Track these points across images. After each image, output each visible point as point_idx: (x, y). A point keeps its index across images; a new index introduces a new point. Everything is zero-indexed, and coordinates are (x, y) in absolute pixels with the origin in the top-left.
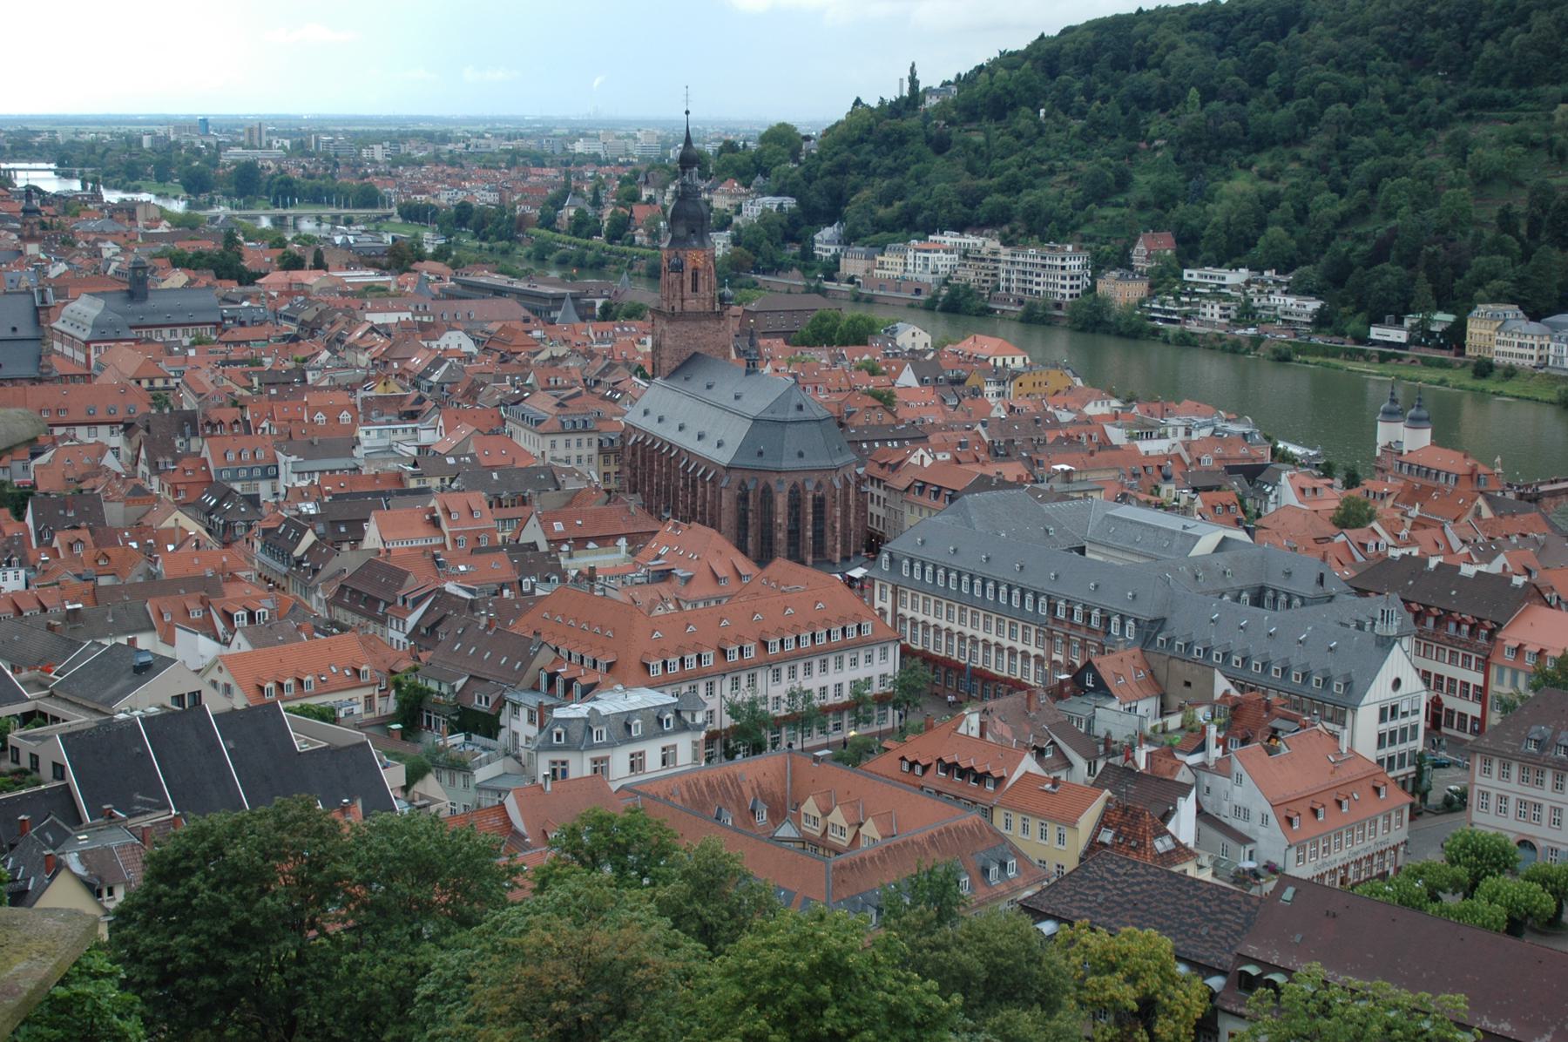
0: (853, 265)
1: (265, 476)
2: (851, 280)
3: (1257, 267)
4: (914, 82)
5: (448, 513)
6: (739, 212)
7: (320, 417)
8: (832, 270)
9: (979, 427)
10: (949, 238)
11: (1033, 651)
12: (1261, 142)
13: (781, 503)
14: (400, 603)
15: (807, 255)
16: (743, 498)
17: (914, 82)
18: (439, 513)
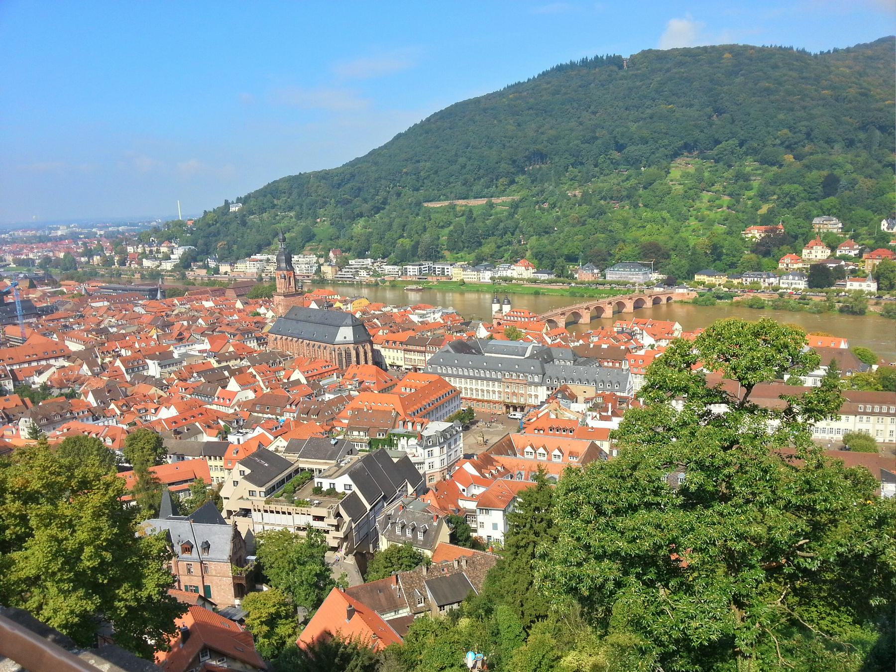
0: (224, 268)
1: (144, 369)
2: (226, 273)
3: (375, 259)
4: (226, 201)
5: (259, 373)
6: (173, 253)
7: (143, 345)
8: (217, 271)
9: (375, 320)
10: (258, 257)
11: (497, 389)
12: (361, 215)
13: (353, 353)
14: (288, 407)
15: (206, 267)
16: (340, 354)
17: (226, 201)
18: (255, 373)
